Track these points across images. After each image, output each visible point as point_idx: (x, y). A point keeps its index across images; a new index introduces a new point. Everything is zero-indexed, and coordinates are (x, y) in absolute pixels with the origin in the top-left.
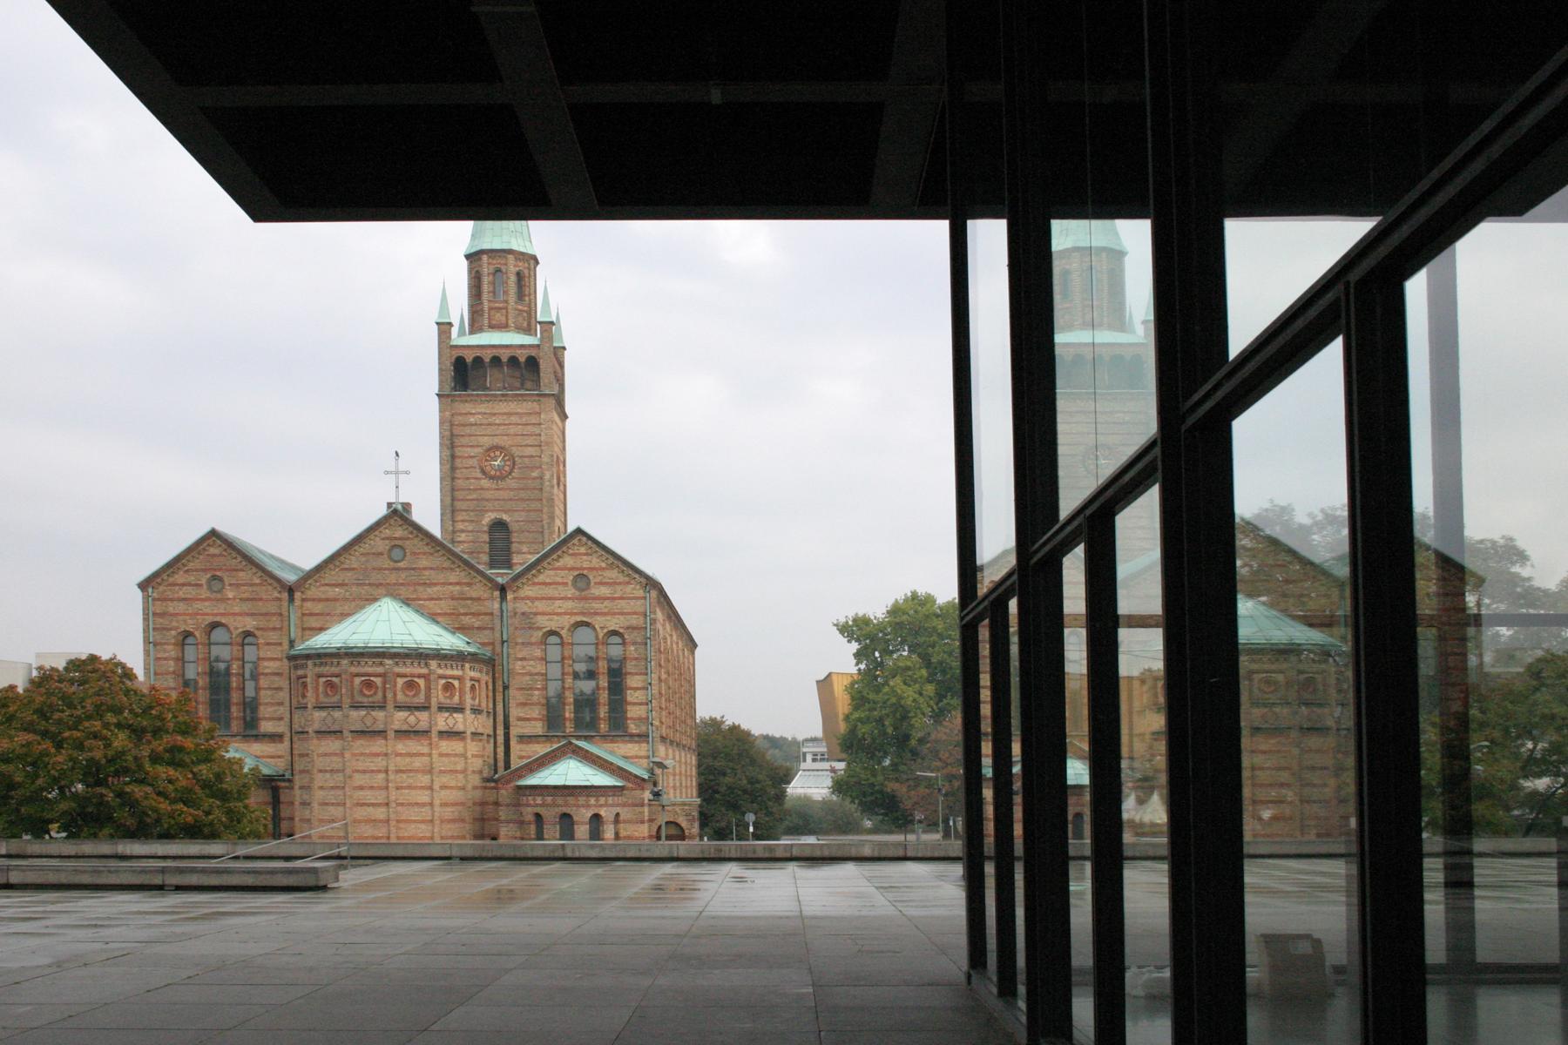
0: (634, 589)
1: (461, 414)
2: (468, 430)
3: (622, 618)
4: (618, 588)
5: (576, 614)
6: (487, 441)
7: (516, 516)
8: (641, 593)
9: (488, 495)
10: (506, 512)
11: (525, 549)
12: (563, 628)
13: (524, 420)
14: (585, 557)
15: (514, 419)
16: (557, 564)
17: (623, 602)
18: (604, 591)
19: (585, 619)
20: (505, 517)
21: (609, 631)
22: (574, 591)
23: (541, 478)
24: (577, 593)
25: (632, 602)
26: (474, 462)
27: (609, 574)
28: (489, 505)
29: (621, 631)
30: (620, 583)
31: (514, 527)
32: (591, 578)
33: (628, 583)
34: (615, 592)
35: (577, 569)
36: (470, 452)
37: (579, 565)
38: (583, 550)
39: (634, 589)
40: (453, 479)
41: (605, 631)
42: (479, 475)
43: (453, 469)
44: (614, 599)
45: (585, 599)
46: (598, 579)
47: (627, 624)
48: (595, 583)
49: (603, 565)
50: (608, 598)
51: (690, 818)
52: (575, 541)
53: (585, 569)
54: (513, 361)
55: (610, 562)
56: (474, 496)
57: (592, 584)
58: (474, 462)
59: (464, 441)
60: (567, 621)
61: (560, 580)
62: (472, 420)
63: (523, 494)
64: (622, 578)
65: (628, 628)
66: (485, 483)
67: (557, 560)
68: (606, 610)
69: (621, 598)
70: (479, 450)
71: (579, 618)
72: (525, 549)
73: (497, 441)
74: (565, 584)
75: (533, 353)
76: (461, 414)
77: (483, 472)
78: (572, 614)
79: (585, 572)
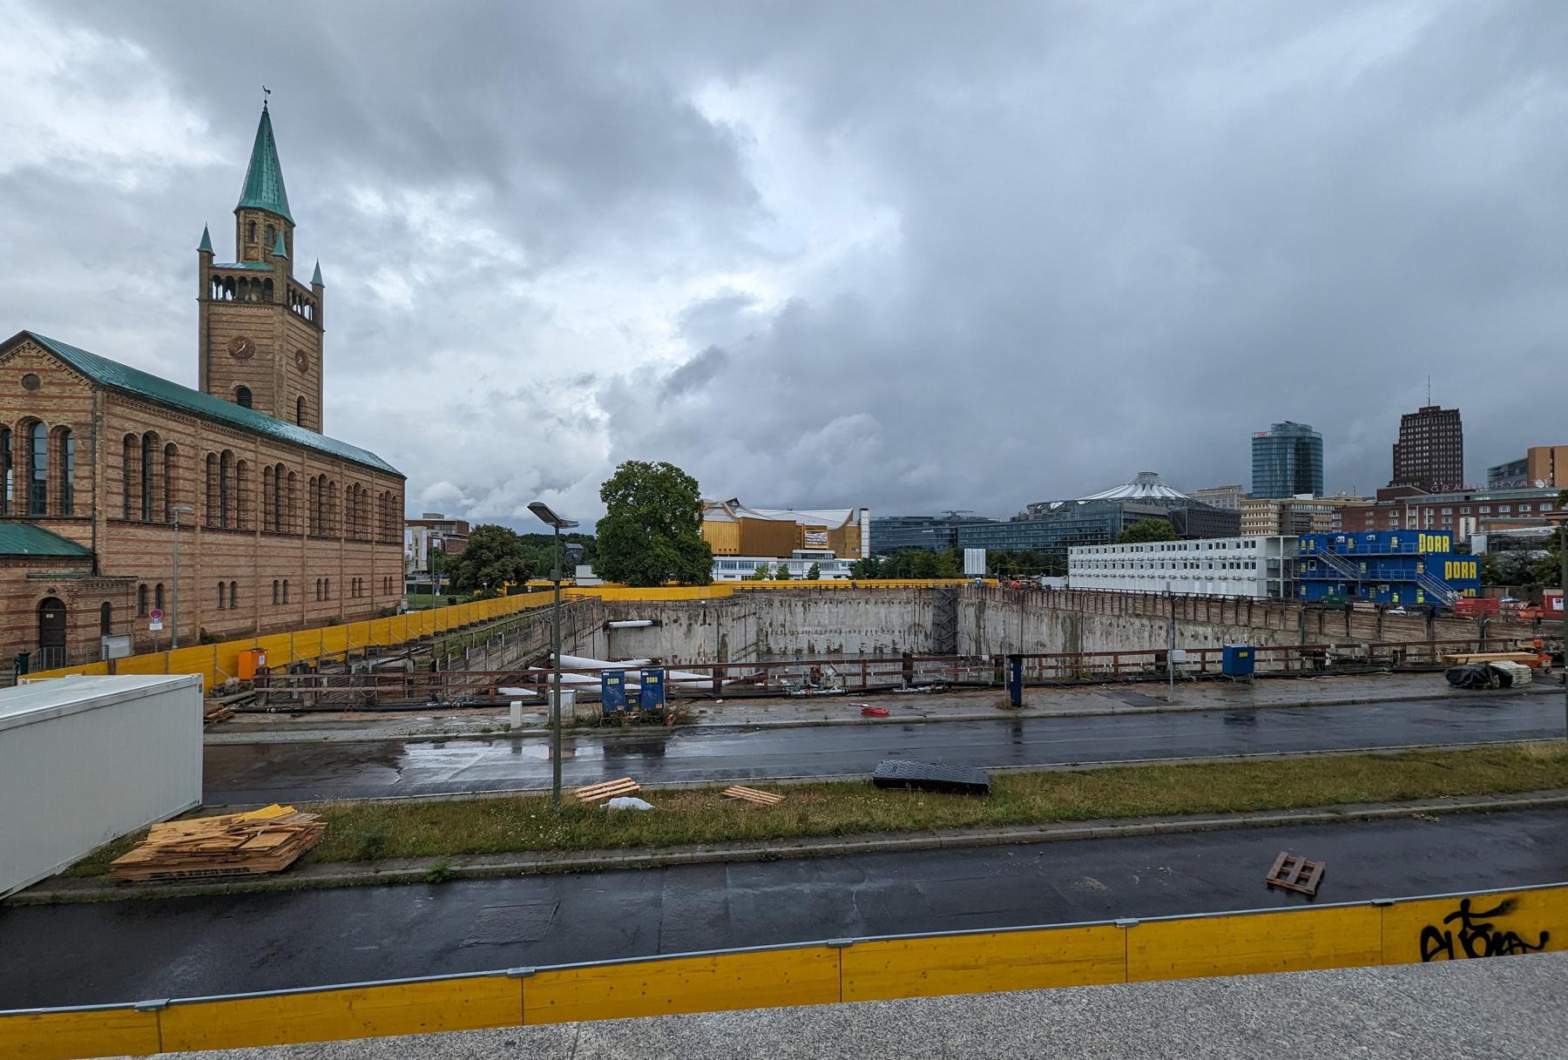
0: (83, 389)
1: (215, 314)
2: (220, 325)
3: (70, 414)
4: (68, 388)
5: (25, 410)
6: (235, 333)
7: (256, 384)
8: (90, 394)
9: (235, 369)
10: (247, 381)
11: (261, 407)
12: (12, 422)
13: (263, 320)
14: (35, 360)
15: (254, 320)
16: (7, 365)
17: (72, 401)
18: (55, 390)
19: (33, 415)
20: (247, 385)
21: (57, 427)
22: (23, 389)
23: (273, 360)
24: (27, 391)
25: (81, 401)
26: (225, 347)
27: (58, 375)
28: (235, 376)
29: (70, 426)
30: (68, 384)
31: (253, 392)
32: (40, 377)
33: (78, 384)
34: (64, 392)
35: (27, 370)
36: (222, 341)
37: (28, 366)
38: (33, 353)
39: (83, 389)
40: (208, 357)
41: (54, 426)
42: (229, 356)
43: (209, 350)
44: (62, 398)
45: (35, 396)
46: (46, 380)
47: (76, 420)
48: (45, 383)
49: (54, 367)
50: (57, 397)
51: (72, 594)
52: (25, 344)
53: (36, 370)
54: (255, 280)
55: (58, 364)
56: (224, 370)
57: (42, 384)
58: (225, 347)
59: (218, 332)
60: (16, 416)
61: (10, 379)
62: (224, 318)
63: (259, 370)
64: (71, 380)
65: (76, 424)
66: (232, 361)
67: (8, 359)
68: (54, 408)
69: (71, 397)
70: (227, 339)
71: (28, 414)
72: (261, 407)
73: (242, 333)
74: (17, 383)
75: (269, 275)
76: (215, 314)
77: (232, 353)
78: (20, 410)
79: (35, 373)
